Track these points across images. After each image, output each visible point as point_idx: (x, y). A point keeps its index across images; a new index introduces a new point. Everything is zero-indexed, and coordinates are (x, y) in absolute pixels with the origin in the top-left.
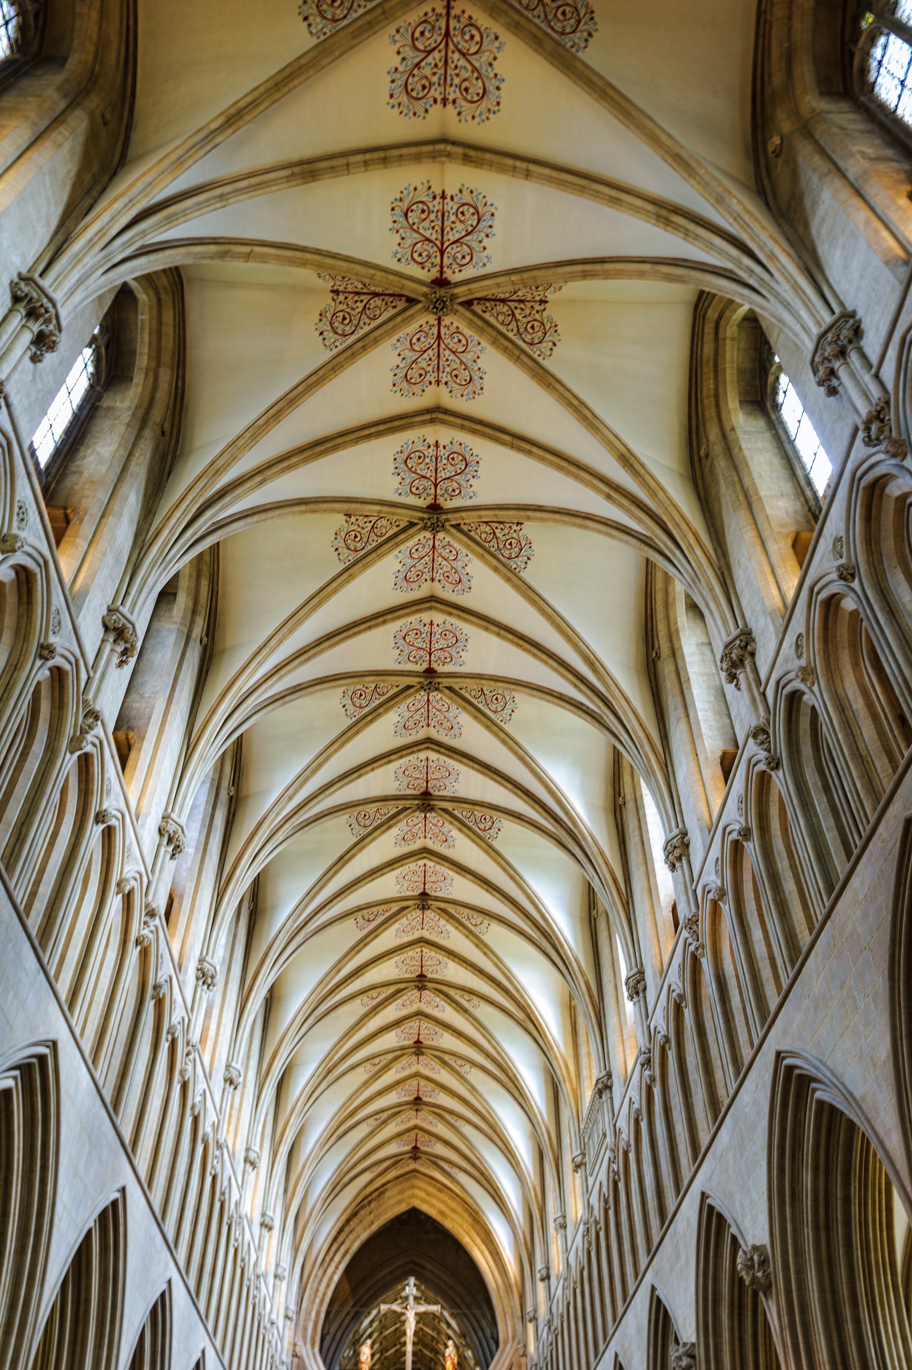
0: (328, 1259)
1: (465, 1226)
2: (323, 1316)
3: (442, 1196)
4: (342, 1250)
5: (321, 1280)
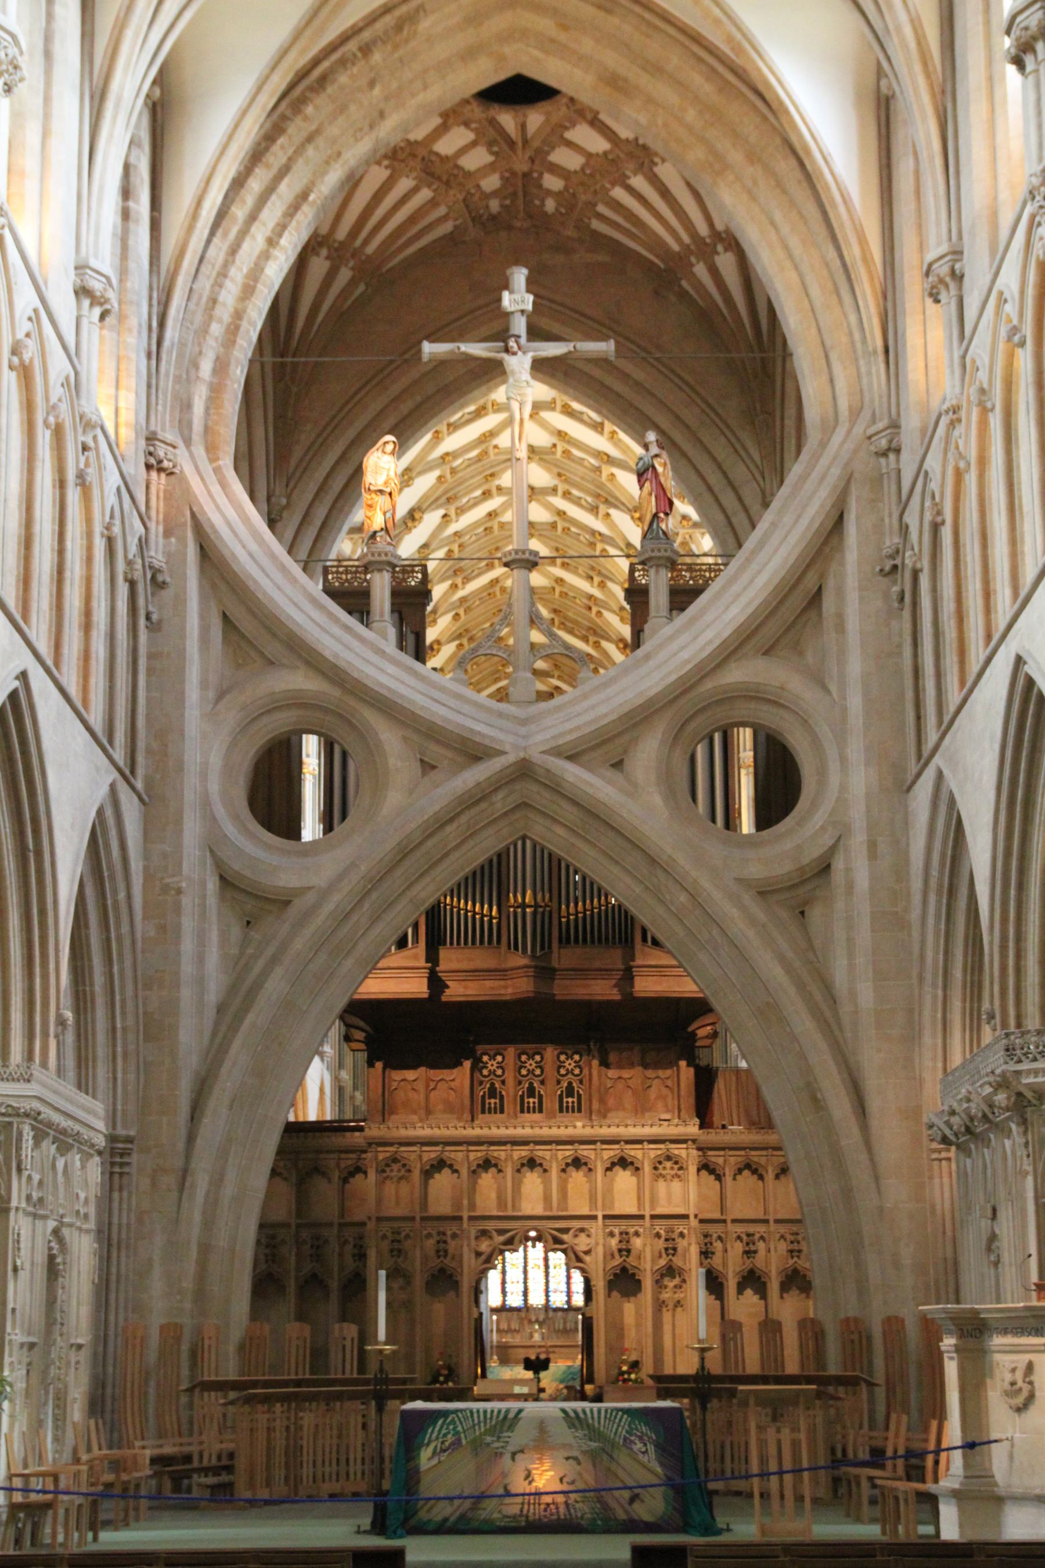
0: (239, 212)
1: (691, 115)
2: (238, 374)
4: (286, 190)
5: (223, 274)
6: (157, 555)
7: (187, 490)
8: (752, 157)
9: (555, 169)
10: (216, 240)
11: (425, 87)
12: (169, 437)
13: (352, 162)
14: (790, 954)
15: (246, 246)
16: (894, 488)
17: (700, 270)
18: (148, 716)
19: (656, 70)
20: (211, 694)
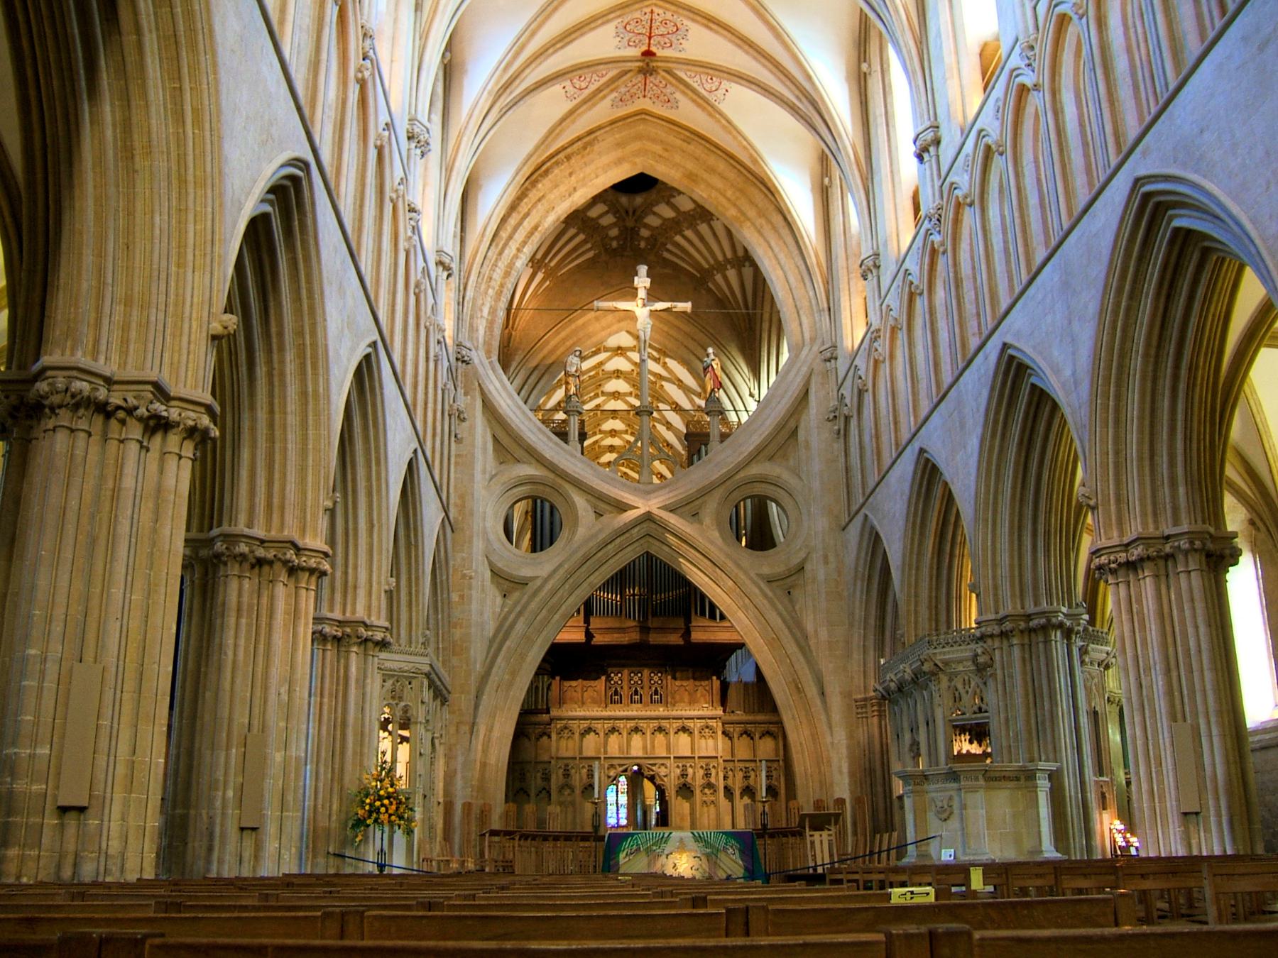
0: (504, 235)
3: (691, 147)
4: (528, 224)
5: (495, 265)
6: (462, 406)
7: (476, 372)
8: (761, 214)
9: (647, 226)
10: (492, 248)
11: (597, 177)
12: (468, 345)
13: (560, 212)
14: (784, 613)
15: (506, 252)
16: (834, 377)
17: (718, 278)
18: (455, 486)
19: (712, 170)
20: (488, 476)
